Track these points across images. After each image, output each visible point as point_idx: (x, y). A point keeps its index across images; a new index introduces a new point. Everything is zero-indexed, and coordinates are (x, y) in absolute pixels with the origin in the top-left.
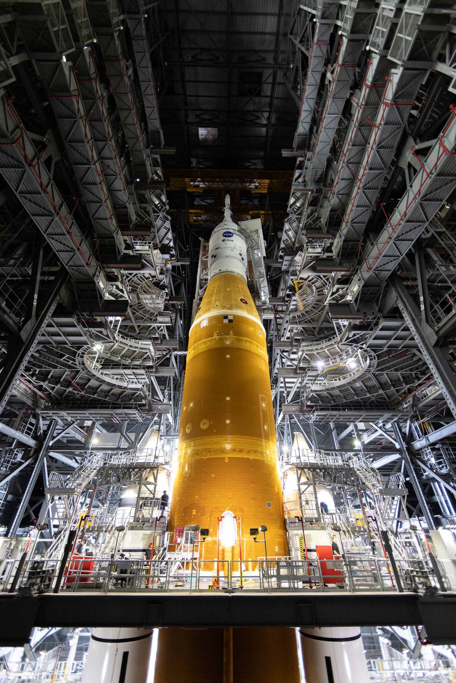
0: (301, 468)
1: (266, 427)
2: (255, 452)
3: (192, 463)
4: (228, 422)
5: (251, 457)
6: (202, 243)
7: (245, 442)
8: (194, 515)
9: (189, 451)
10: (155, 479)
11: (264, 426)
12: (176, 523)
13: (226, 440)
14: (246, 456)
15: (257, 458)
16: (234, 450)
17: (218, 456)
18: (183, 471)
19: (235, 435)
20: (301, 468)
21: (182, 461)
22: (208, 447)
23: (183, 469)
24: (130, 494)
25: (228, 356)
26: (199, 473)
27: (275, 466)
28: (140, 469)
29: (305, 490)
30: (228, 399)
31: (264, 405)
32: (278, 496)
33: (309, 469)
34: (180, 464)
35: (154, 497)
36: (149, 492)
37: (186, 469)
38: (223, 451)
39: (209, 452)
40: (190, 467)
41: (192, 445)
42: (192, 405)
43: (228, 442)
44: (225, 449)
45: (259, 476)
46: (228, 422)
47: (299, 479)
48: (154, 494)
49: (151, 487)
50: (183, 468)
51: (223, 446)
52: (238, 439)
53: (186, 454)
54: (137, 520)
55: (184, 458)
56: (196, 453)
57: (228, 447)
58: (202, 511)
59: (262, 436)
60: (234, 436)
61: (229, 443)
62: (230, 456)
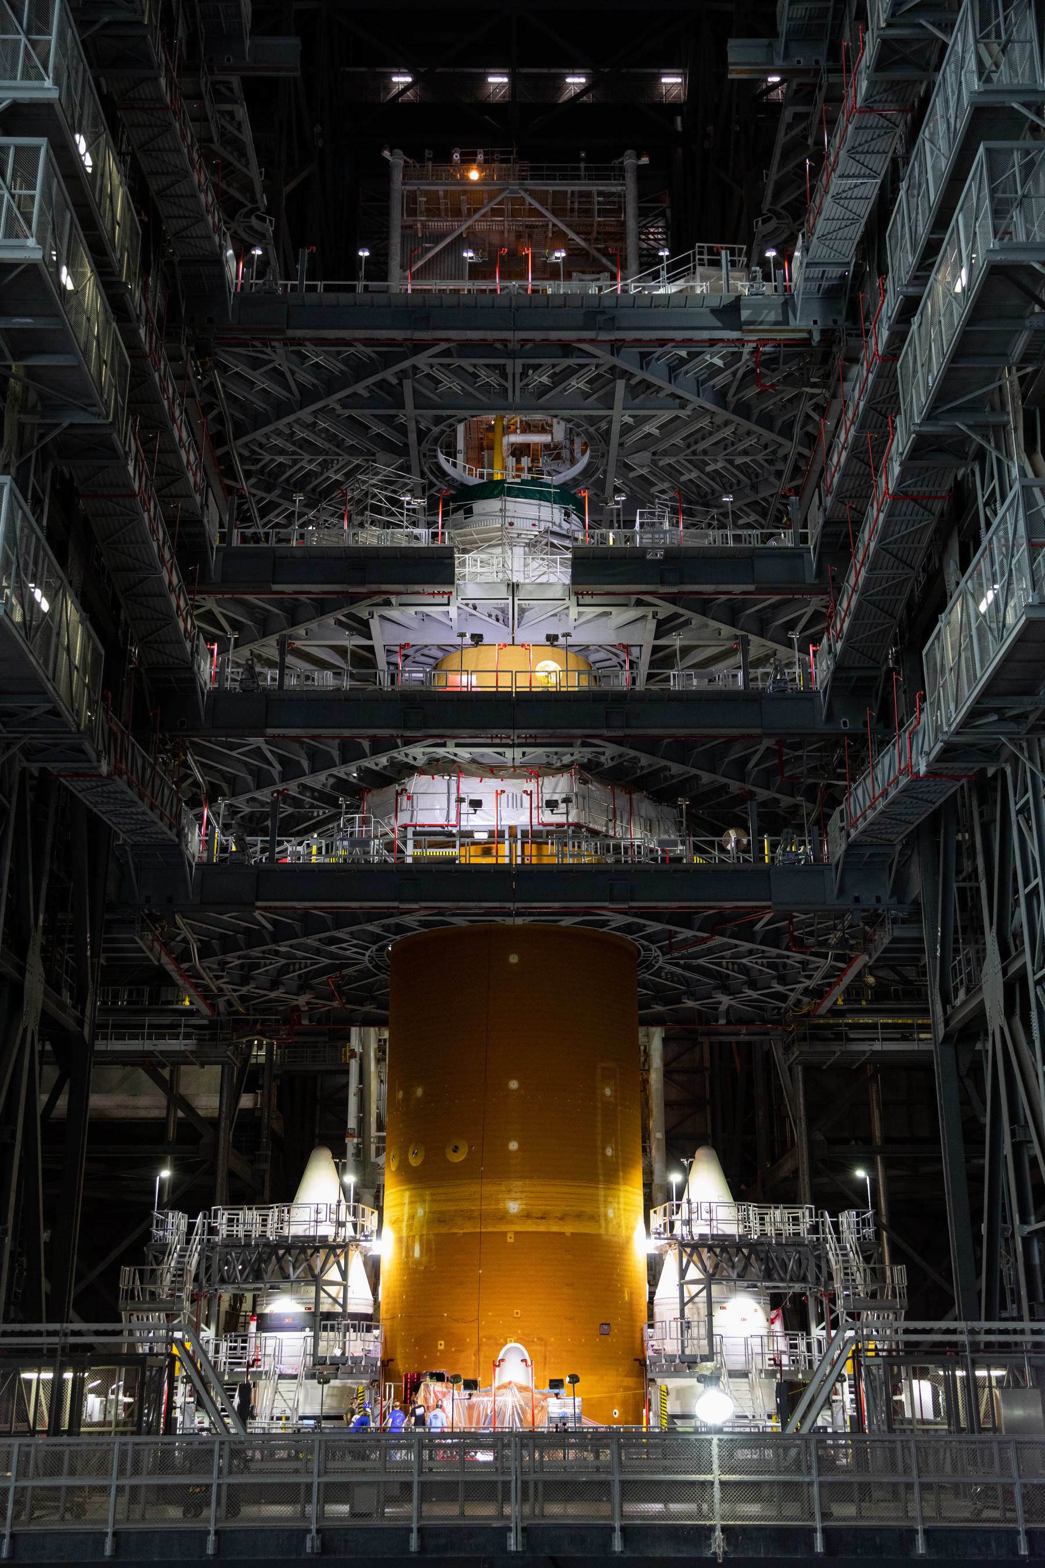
0: (692, 1247)
1: (609, 1152)
2: (579, 1216)
3: (429, 1242)
4: (513, 1146)
5: (568, 1229)
6: (397, 177)
7: (554, 1194)
8: (441, 1351)
9: (420, 1212)
10: (344, 1274)
11: (604, 1149)
12: (402, 1366)
13: (509, 1191)
14: (555, 1229)
15: (583, 1231)
16: (527, 1216)
17: (491, 1229)
18: (407, 1256)
19: (531, 1178)
20: (692, 1247)
21: (404, 1234)
22: (465, 1206)
23: (407, 1252)
24: (284, 1305)
25: (514, 959)
26: (445, 1265)
27: (628, 1240)
28: (303, 1250)
29: (696, 1295)
30: (514, 1085)
31: (608, 1092)
32: (631, 1309)
33: (711, 1249)
34: (400, 1240)
35: (345, 1310)
36: (330, 1300)
37: (417, 1253)
38: (503, 1217)
39: (470, 1218)
40: (426, 1249)
41: (428, 1198)
42: (419, 1092)
43: (514, 1195)
44: (507, 1212)
45: (592, 1264)
46: (513, 1146)
47: (683, 1272)
48: (344, 1306)
49: (333, 1290)
50: (409, 1250)
51: (501, 1206)
52: (539, 1189)
53: (412, 1217)
54: (319, 1361)
55: (410, 1226)
56: (437, 1219)
57: (514, 1207)
58: (457, 1342)
59: (597, 1174)
60: (528, 1182)
61: (515, 1199)
62: (518, 1228)
